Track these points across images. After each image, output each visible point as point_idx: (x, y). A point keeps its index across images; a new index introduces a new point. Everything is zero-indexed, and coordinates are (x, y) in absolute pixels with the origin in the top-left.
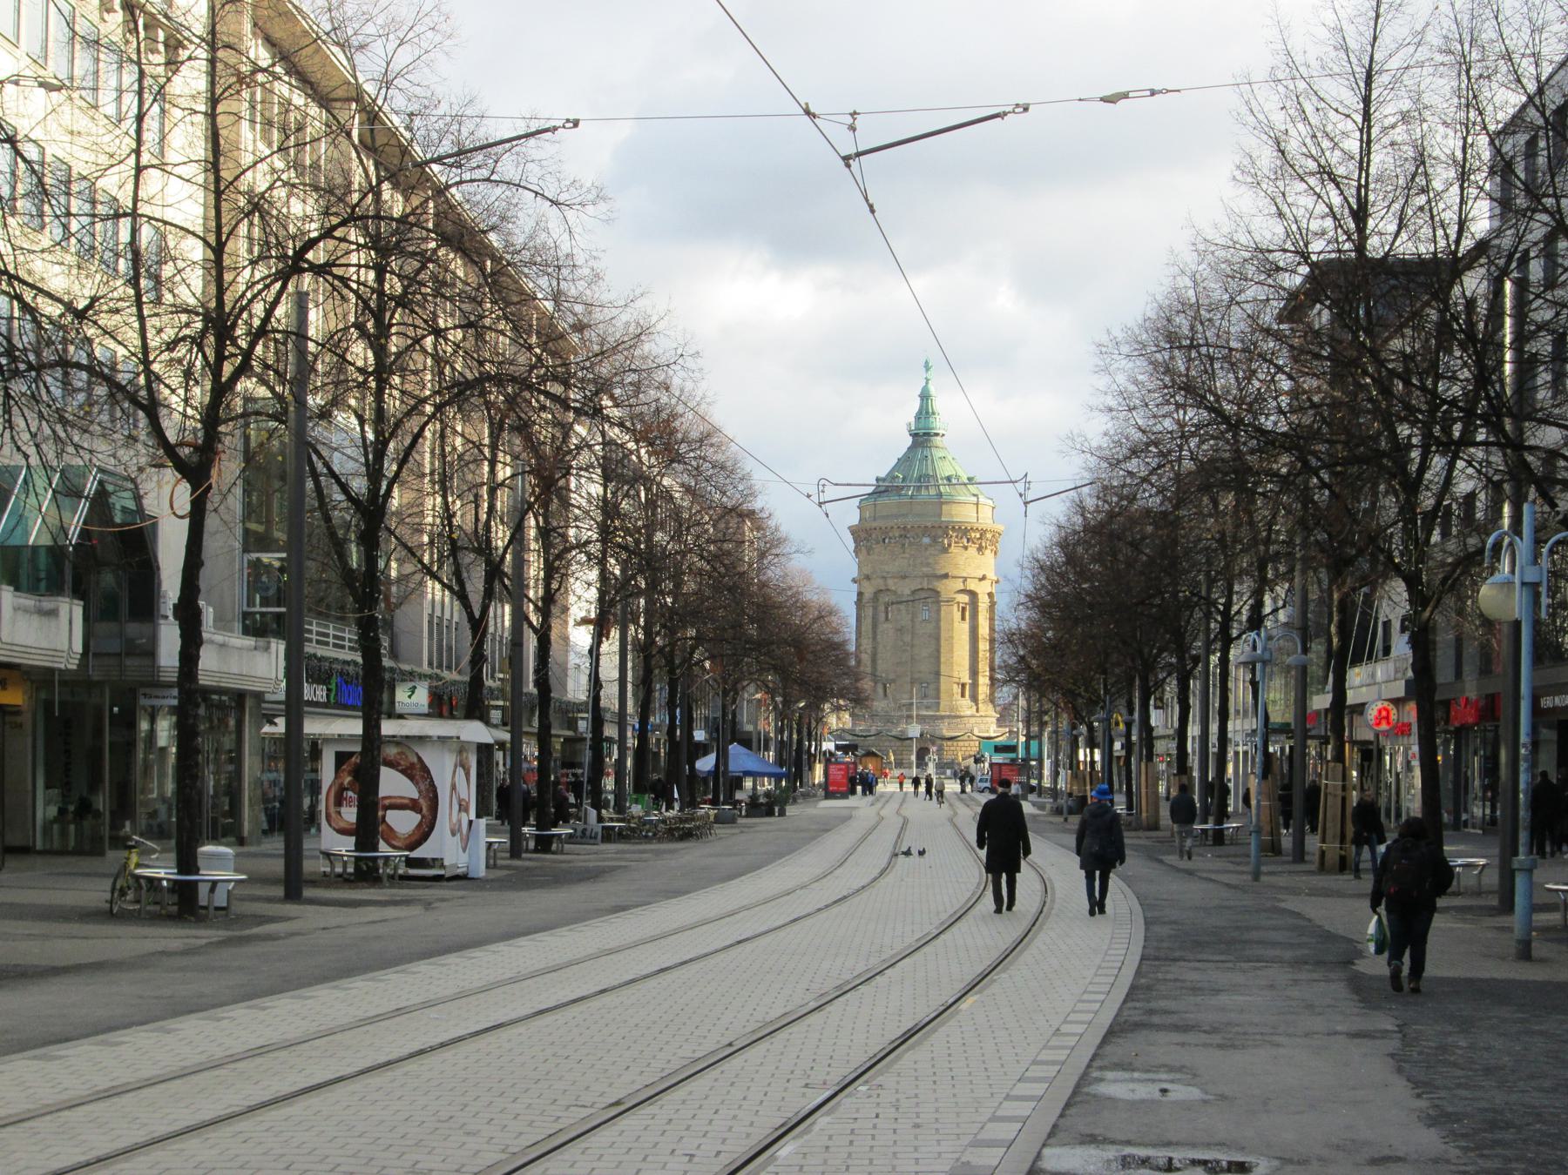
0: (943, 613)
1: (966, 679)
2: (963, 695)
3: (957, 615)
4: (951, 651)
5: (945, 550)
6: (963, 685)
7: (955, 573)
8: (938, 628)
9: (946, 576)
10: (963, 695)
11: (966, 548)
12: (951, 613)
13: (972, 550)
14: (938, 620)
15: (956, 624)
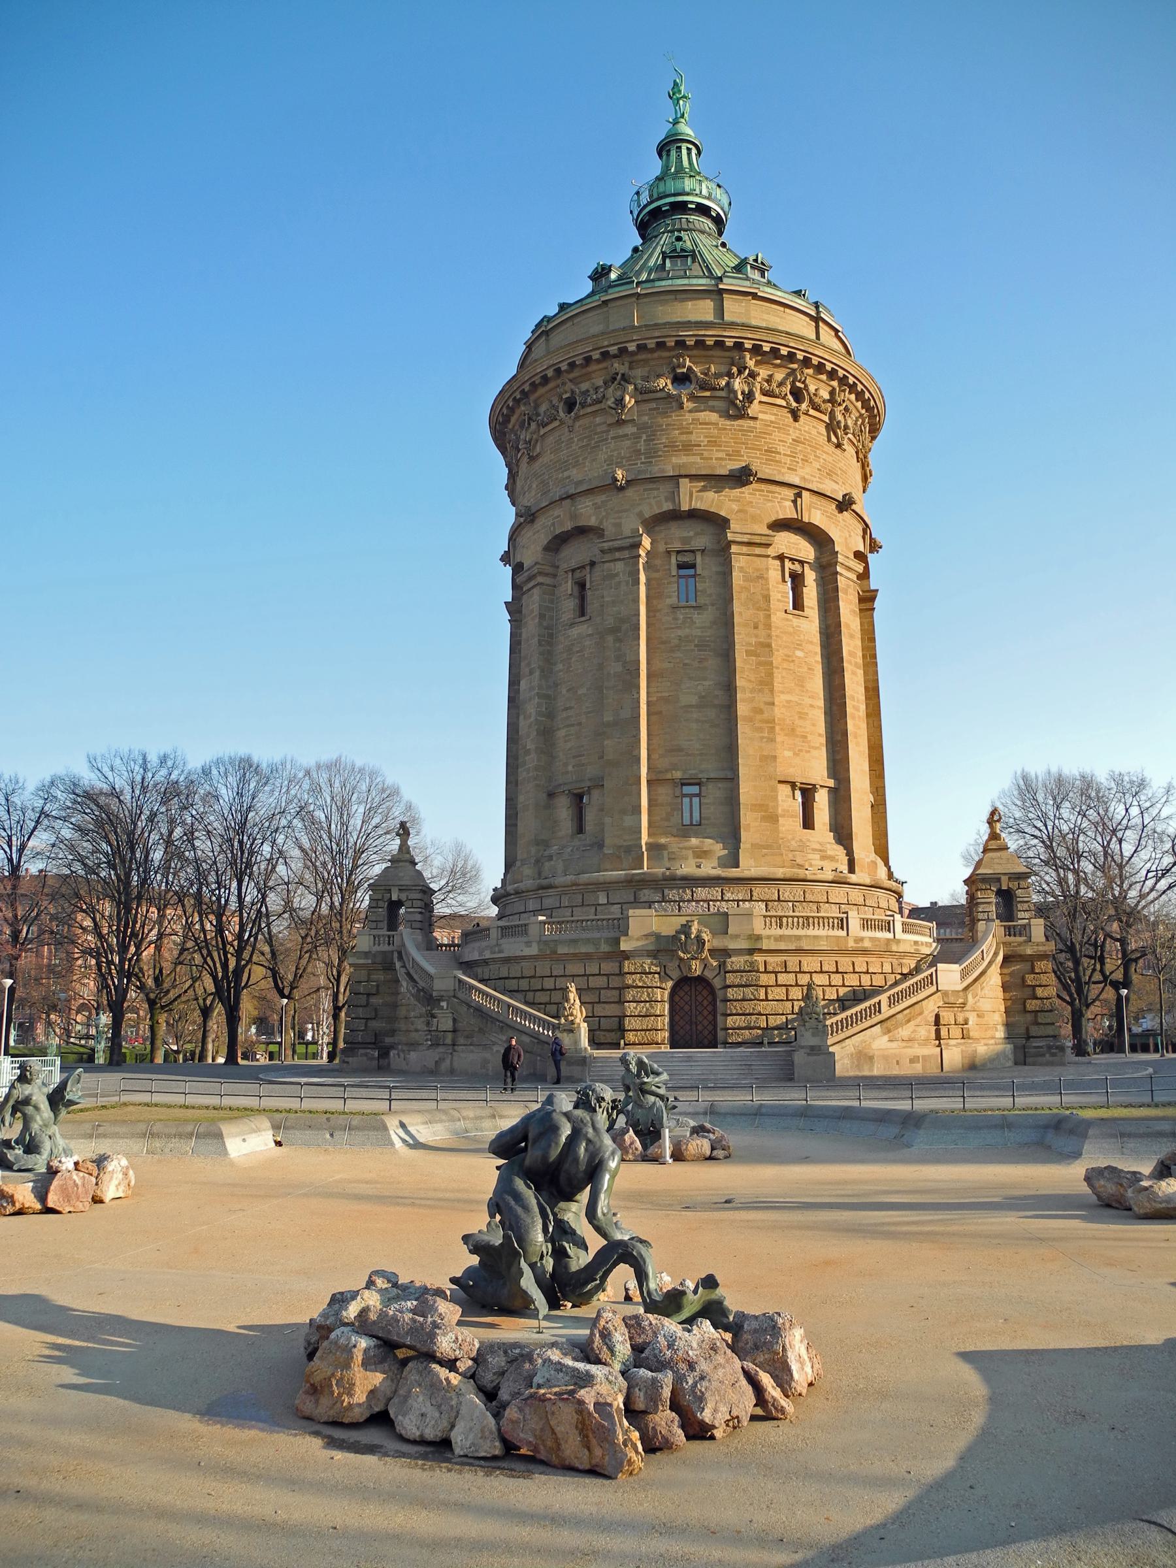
0: (737, 578)
1: (817, 770)
2: (808, 823)
3: (782, 593)
4: (766, 683)
5: (736, 409)
6: (808, 793)
7: (765, 471)
8: (726, 622)
9: (742, 477)
10: (808, 823)
11: (795, 415)
12: (762, 577)
13: (812, 427)
14: (726, 599)
15: (777, 617)
